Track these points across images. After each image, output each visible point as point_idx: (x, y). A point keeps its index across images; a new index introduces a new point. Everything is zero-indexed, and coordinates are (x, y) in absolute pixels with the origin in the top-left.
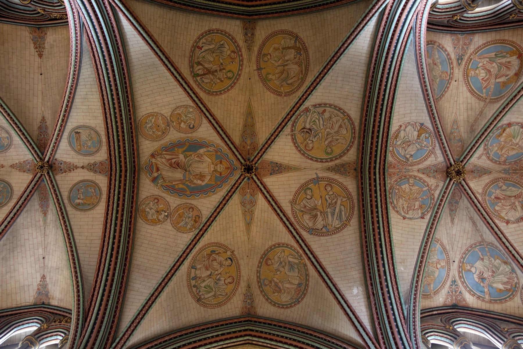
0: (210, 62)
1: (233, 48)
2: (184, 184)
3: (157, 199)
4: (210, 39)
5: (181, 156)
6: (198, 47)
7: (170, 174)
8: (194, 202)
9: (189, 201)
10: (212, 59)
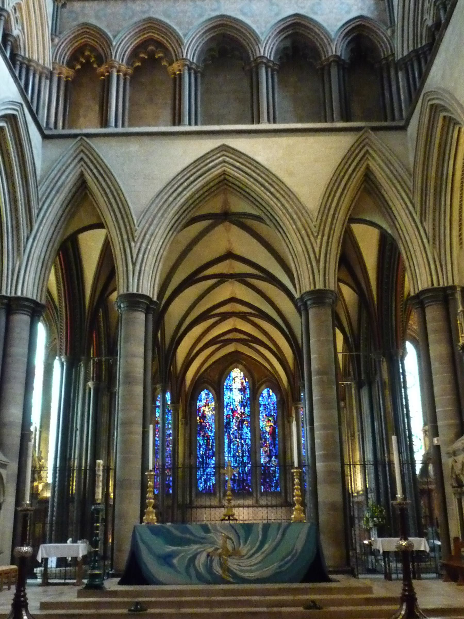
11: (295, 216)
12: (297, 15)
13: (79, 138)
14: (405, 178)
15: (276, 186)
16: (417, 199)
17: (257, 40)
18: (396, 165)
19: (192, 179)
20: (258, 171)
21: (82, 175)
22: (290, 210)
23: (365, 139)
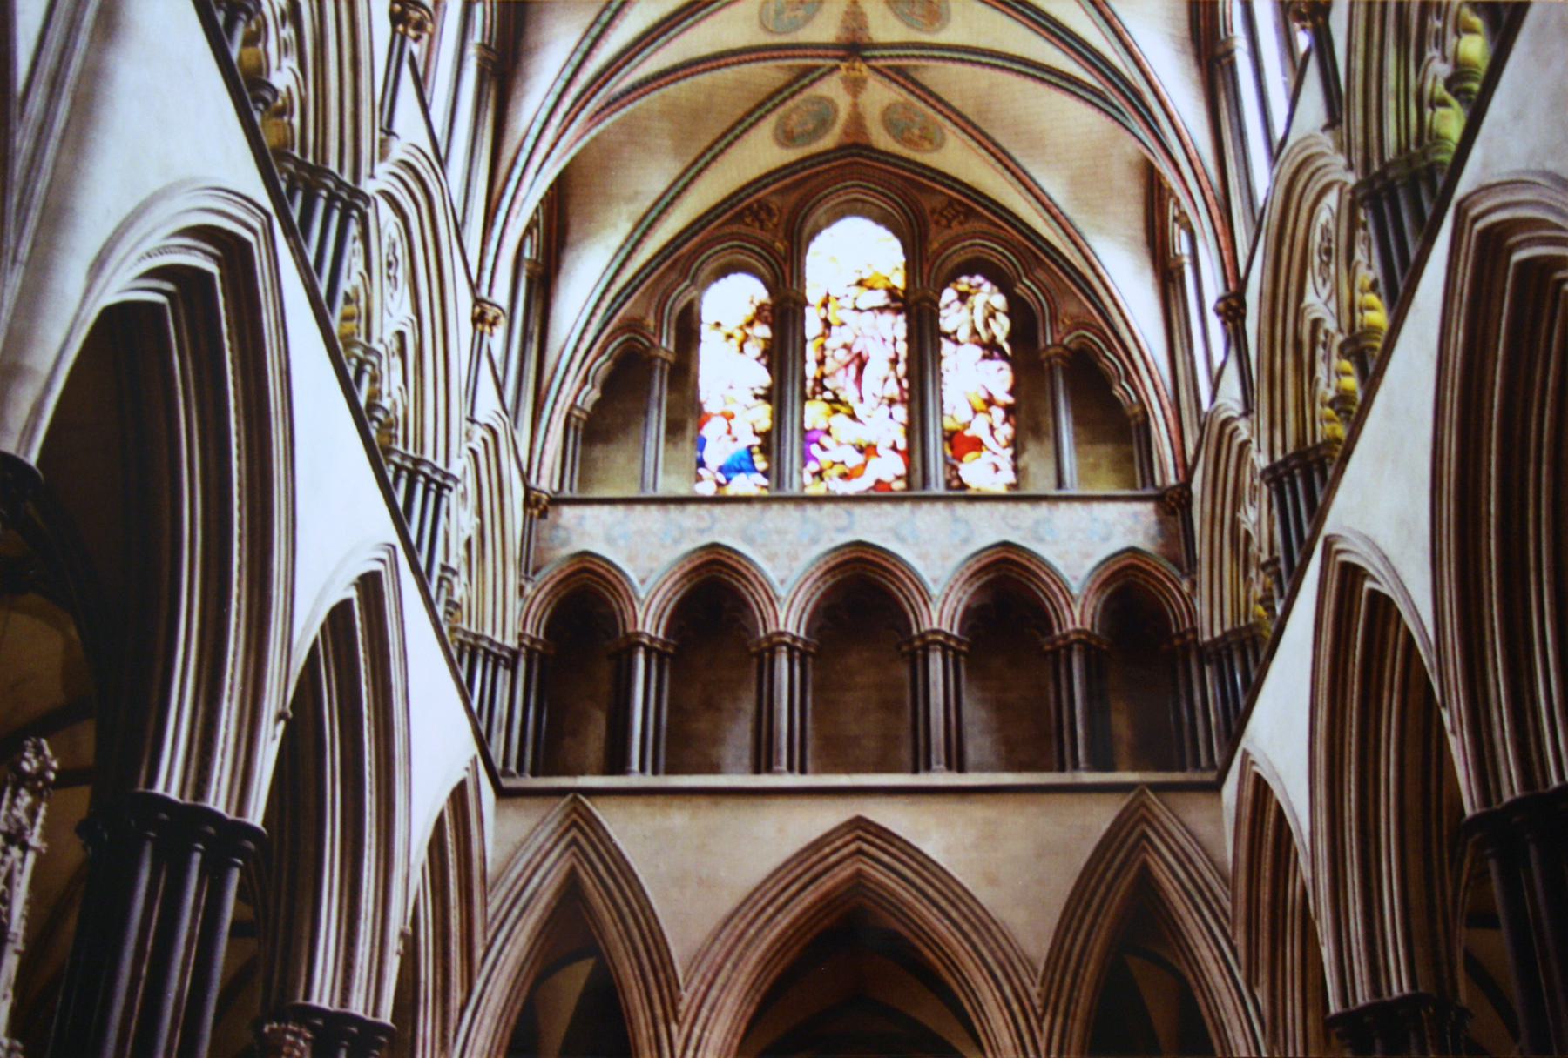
11: (999, 973)
12: (1006, 545)
13: (570, 796)
14: (1218, 891)
15: (963, 907)
16: (1240, 941)
17: (926, 598)
18: (1200, 865)
19: (794, 888)
20: (926, 874)
22: (990, 960)
23: (1138, 808)
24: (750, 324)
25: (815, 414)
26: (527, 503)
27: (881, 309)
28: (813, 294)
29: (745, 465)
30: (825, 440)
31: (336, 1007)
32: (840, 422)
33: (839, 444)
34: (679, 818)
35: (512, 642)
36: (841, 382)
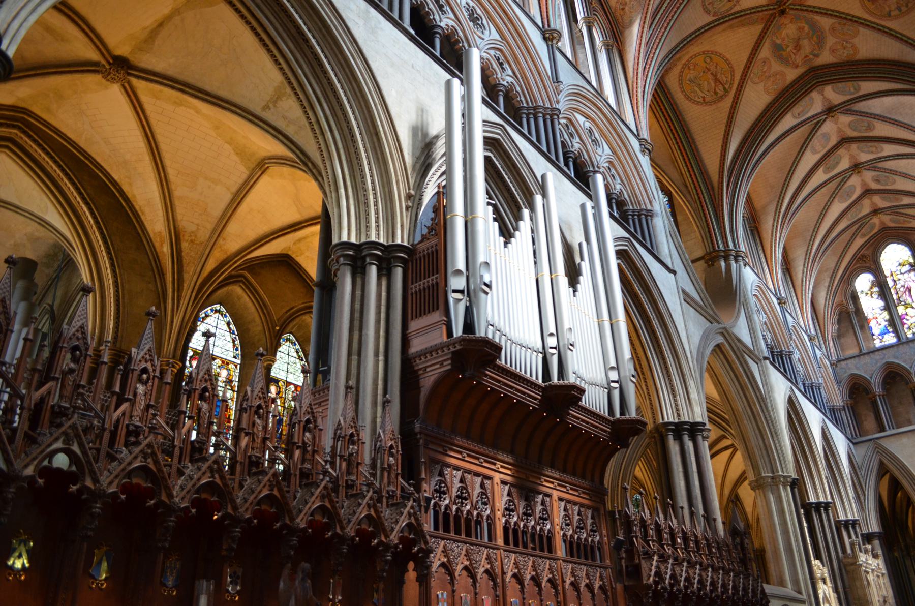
0: (709, 83)
1: (686, 71)
2: (812, 38)
3: (833, 51)
4: (693, 94)
5: (788, 50)
6: (704, 100)
7: (807, 48)
8: (827, 28)
9: (827, 32)
10: (706, 83)
21: (880, 459)
24: (871, 288)
25: (901, 310)
26: (831, 365)
27: (909, 271)
28: (887, 273)
29: (886, 331)
30: (907, 317)
31: (816, 501)
32: (909, 310)
33: (912, 317)
34: (905, 440)
35: (842, 404)
36: (906, 297)
